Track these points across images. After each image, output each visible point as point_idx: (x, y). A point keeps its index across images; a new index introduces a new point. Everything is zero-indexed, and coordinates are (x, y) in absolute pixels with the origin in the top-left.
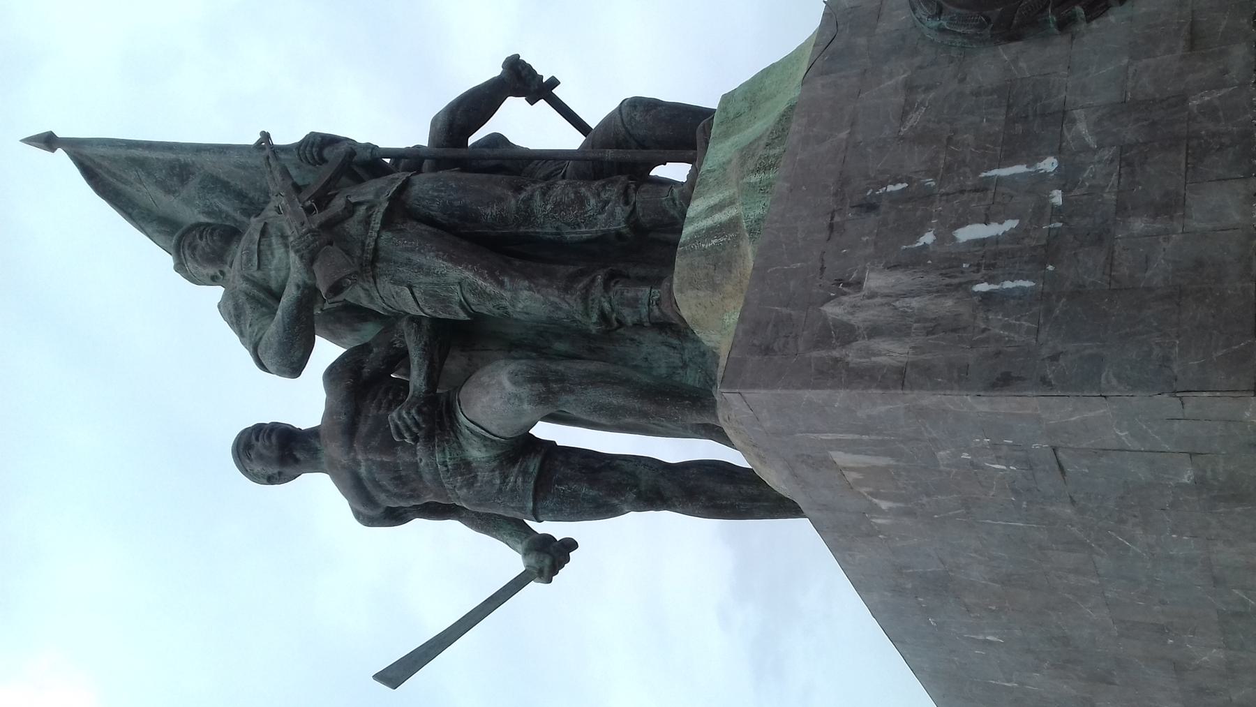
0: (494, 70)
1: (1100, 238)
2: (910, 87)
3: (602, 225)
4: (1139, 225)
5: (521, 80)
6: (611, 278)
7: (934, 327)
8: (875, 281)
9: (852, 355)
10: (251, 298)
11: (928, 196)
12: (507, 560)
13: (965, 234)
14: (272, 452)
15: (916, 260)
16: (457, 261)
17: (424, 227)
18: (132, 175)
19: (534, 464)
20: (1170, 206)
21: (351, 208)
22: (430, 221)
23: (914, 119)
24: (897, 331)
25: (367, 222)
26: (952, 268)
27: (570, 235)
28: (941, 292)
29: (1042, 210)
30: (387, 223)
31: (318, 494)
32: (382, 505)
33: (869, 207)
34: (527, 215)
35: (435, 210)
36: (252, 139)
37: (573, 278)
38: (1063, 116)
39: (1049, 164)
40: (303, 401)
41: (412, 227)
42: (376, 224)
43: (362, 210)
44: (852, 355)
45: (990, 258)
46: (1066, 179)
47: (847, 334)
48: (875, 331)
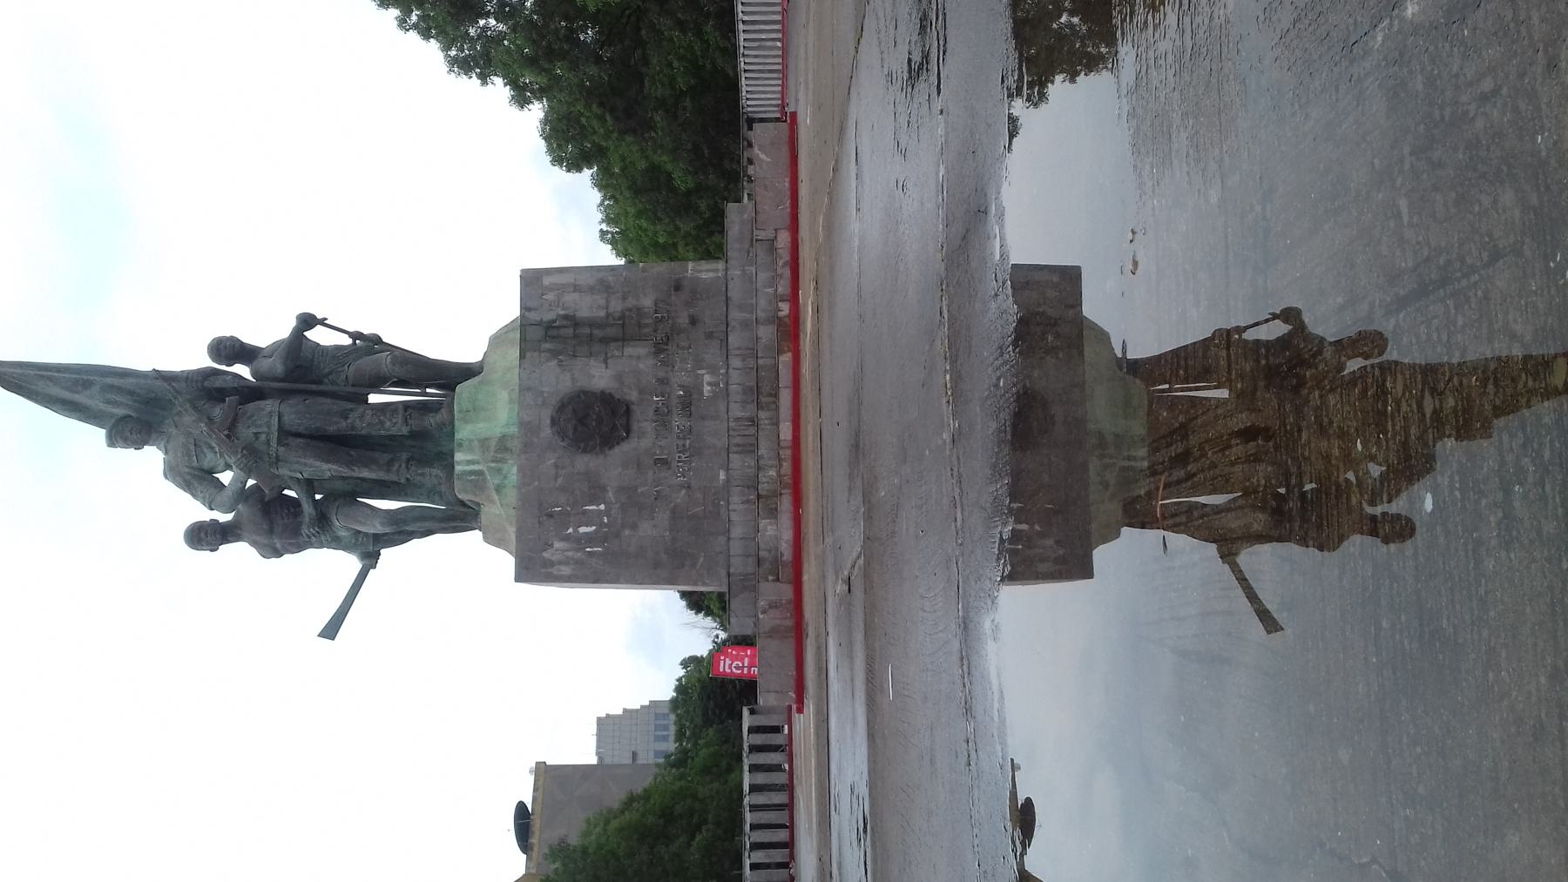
0: (293, 323)
1: (618, 535)
2: (556, 466)
3: (394, 431)
4: (627, 532)
5: (307, 321)
7: (578, 562)
8: (557, 545)
9: (554, 571)
10: (194, 476)
11: (568, 514)
12: (345, 564)
13: (583, 530)
14: (204, 537)
15: (567, 538)
16: (328, 462)
17: (299, 440)
18: (41, 383)
20: (634, 527)
21: (257, 435)
22: (298, 435)
23: (560, 480)
24: (565, 562)
25: (268, 442)
26: (581, 542)
28: (577, 550)
29: (602, 524)
30: (279, 442)
31: (240, 552)
33: (550, 516)
34: (353, 428)
35: (301, 430)
38: (604, 489)
39: (602, 507)
41: (291, 440)
42: (274, 443)
43: (263, 437)
44: (554, 571)
45: (590, 539)
46: (607, 513)
47: (552, 564)
48: (560, 563)
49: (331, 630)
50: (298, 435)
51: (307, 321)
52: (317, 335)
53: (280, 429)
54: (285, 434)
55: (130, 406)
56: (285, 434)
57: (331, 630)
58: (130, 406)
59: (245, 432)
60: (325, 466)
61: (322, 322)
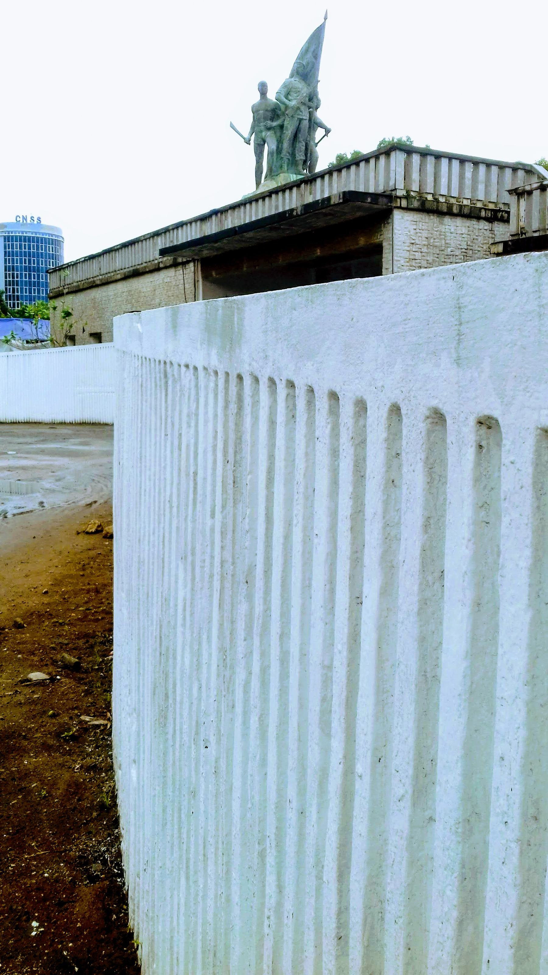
0: (329, 126)
3: (297, 155)
5: (328, 131)
6: (289, 159)
19: (262, 143)
22: (299, 124)
25: (298, 115)
27: (296, 149)
30: (298, 118)
31: (256, 98)
32: (255, 111)
34: (300, 142)
35: (301, 126)
36: (319, 79)
37: (289, 153)
40: (272, 96)
42: (299, 117)
43: (301, 113)
49: (232, 126)
50: (299, 124)
51: (328, 131)
52: (319, 133)
53: (302, 119)
54: (300, 120)
55: (306, 70)
56: (300, 120)
57: (232, 126)
58: (306, 70)
59: (303, 108)
60: (290, 132)
61: (326, 135)
